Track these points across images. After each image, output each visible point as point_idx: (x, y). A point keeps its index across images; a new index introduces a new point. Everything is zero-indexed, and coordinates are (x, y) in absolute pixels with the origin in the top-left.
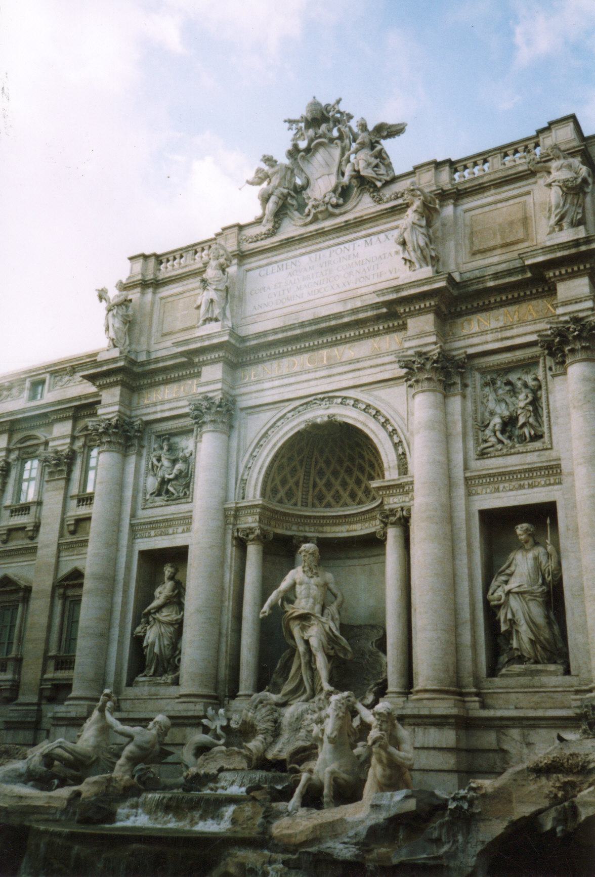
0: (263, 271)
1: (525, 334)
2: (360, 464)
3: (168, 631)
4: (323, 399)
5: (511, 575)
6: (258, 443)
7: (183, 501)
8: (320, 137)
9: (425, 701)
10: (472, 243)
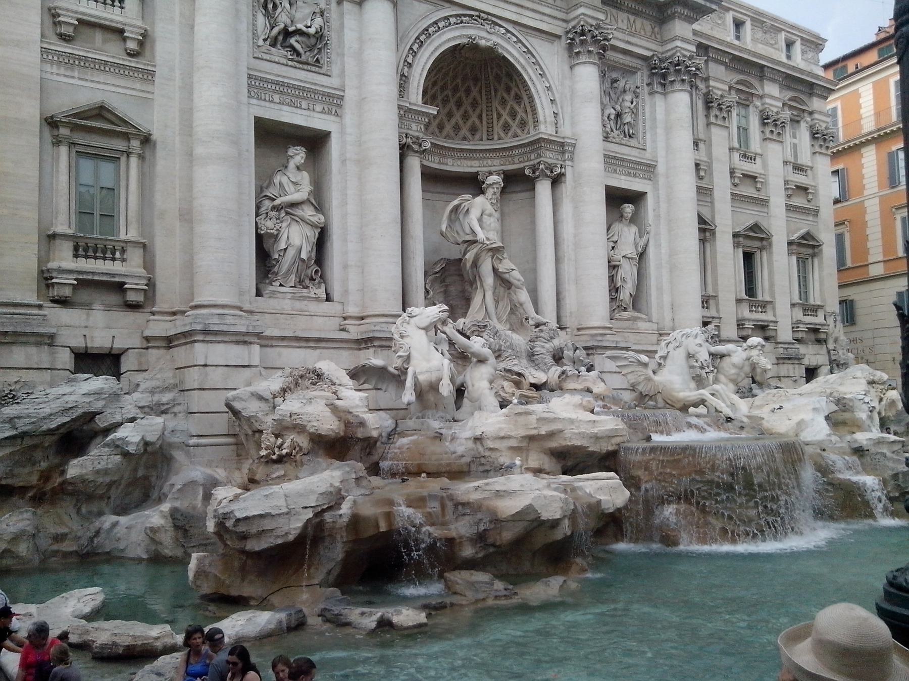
1: (641, 46)
2: (460, 98)
3: (313, 235)
6: (418, 38)
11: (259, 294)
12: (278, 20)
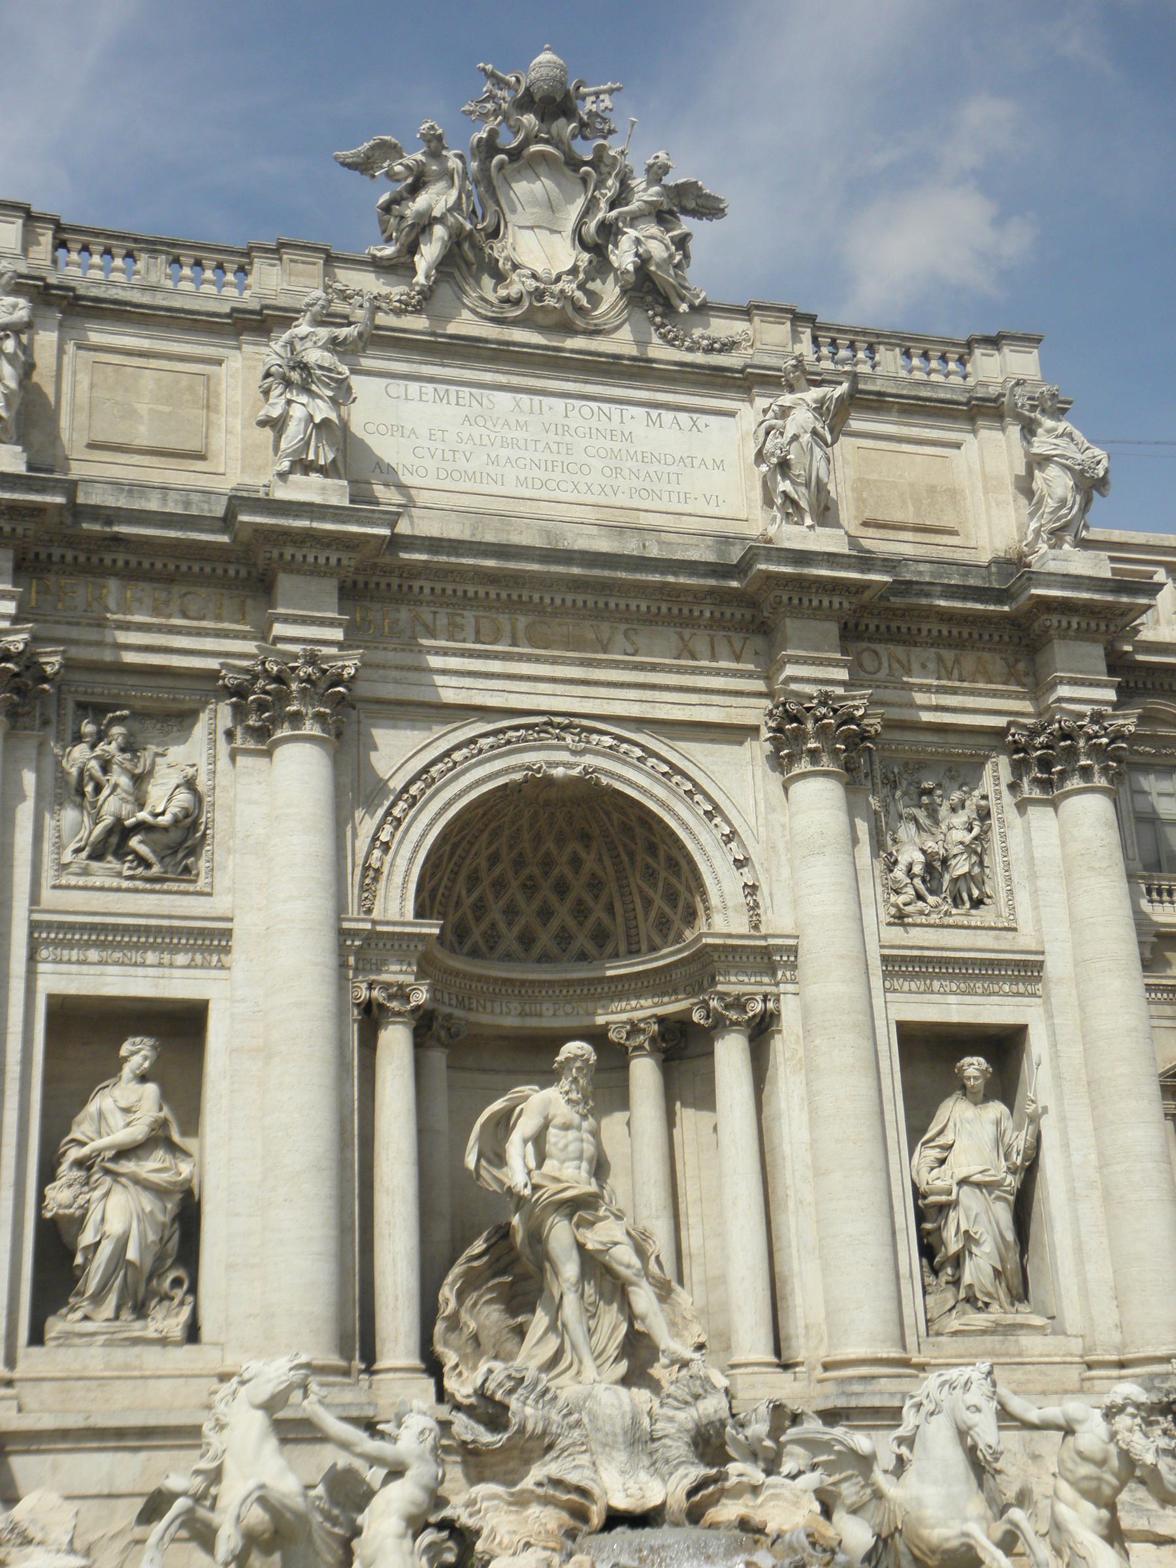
0: (397, 387)
4: (564, 728)
5: (949, 1148)
7: (183, 886)
8: (547, 142)
9: (883, 1381)
10: (860, 501)
11: (37, 1337)
12: (103, 812)
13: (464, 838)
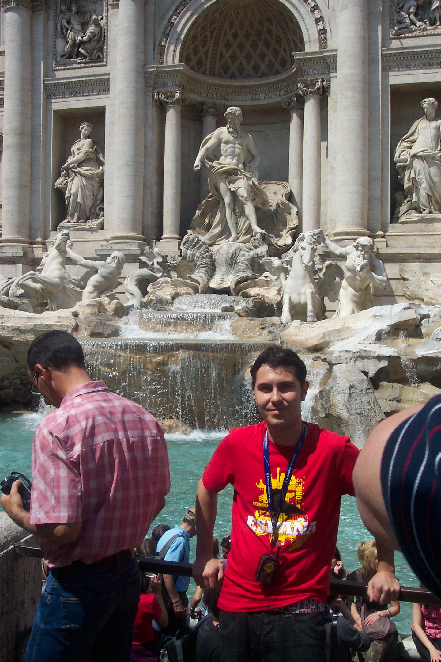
5: (414, 142)
13: (215, 28)
